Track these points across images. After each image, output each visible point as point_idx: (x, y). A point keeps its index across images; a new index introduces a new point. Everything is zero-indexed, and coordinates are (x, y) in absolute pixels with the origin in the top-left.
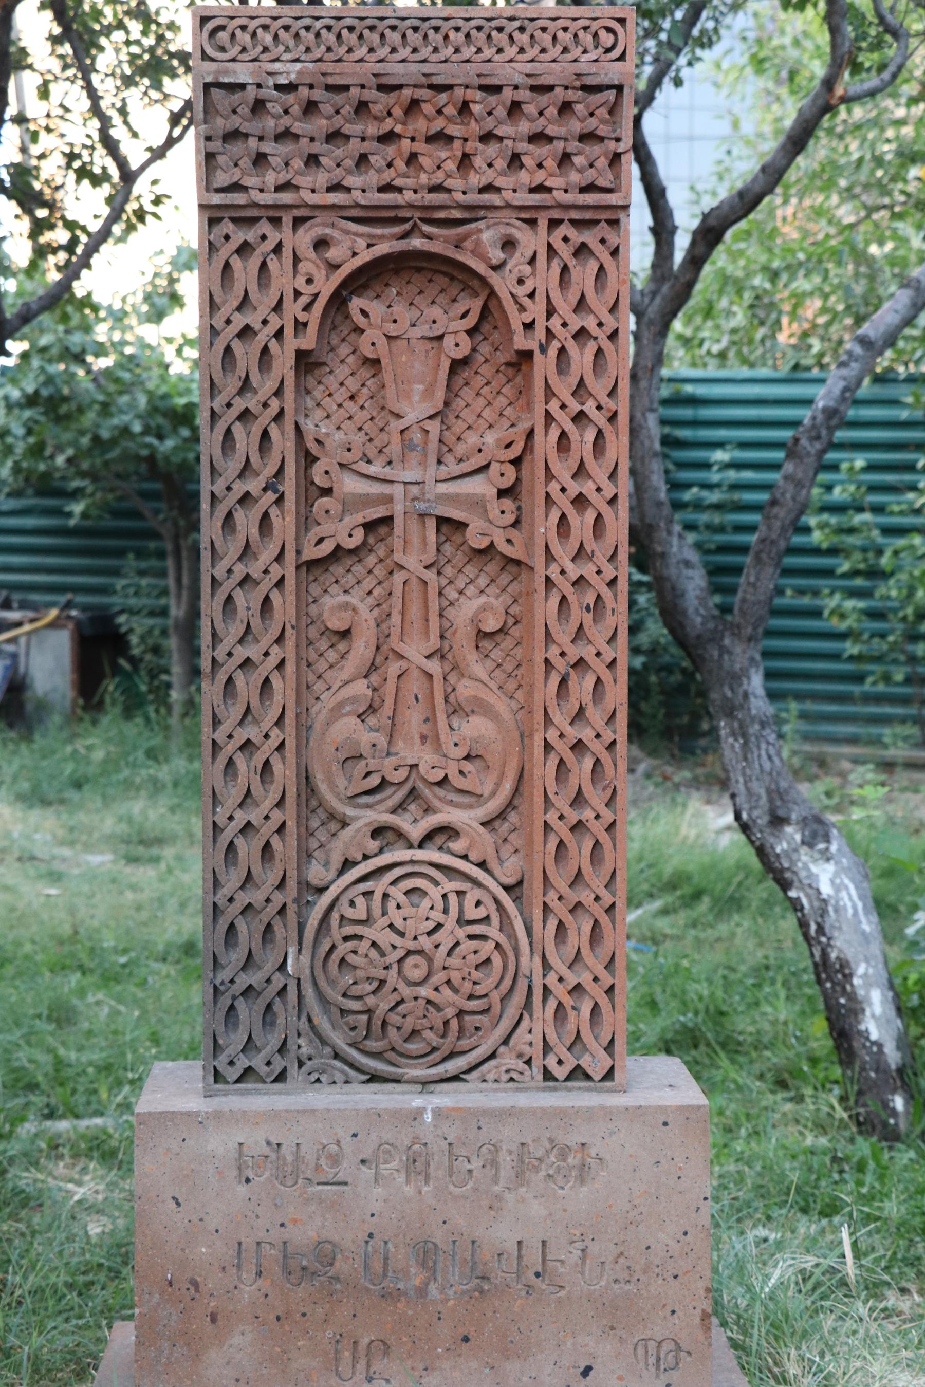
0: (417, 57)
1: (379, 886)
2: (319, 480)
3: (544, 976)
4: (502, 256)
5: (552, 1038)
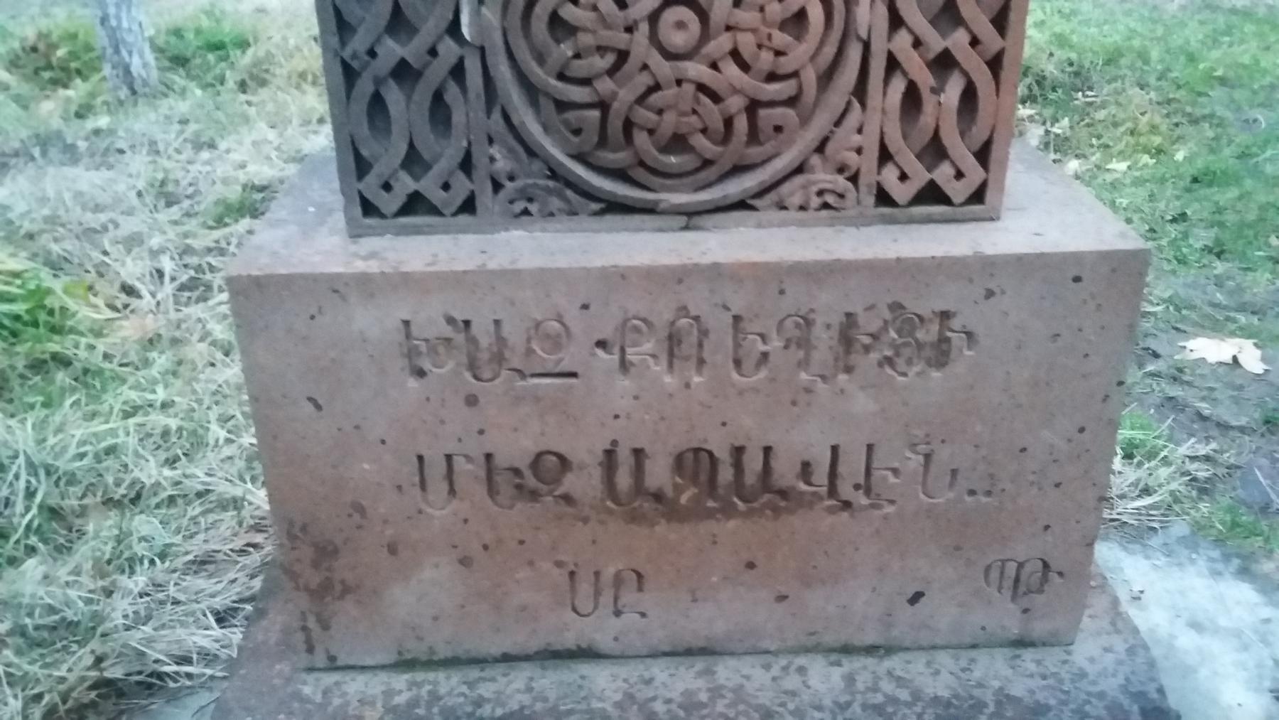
3: (889, 39)
5: (895, 142)
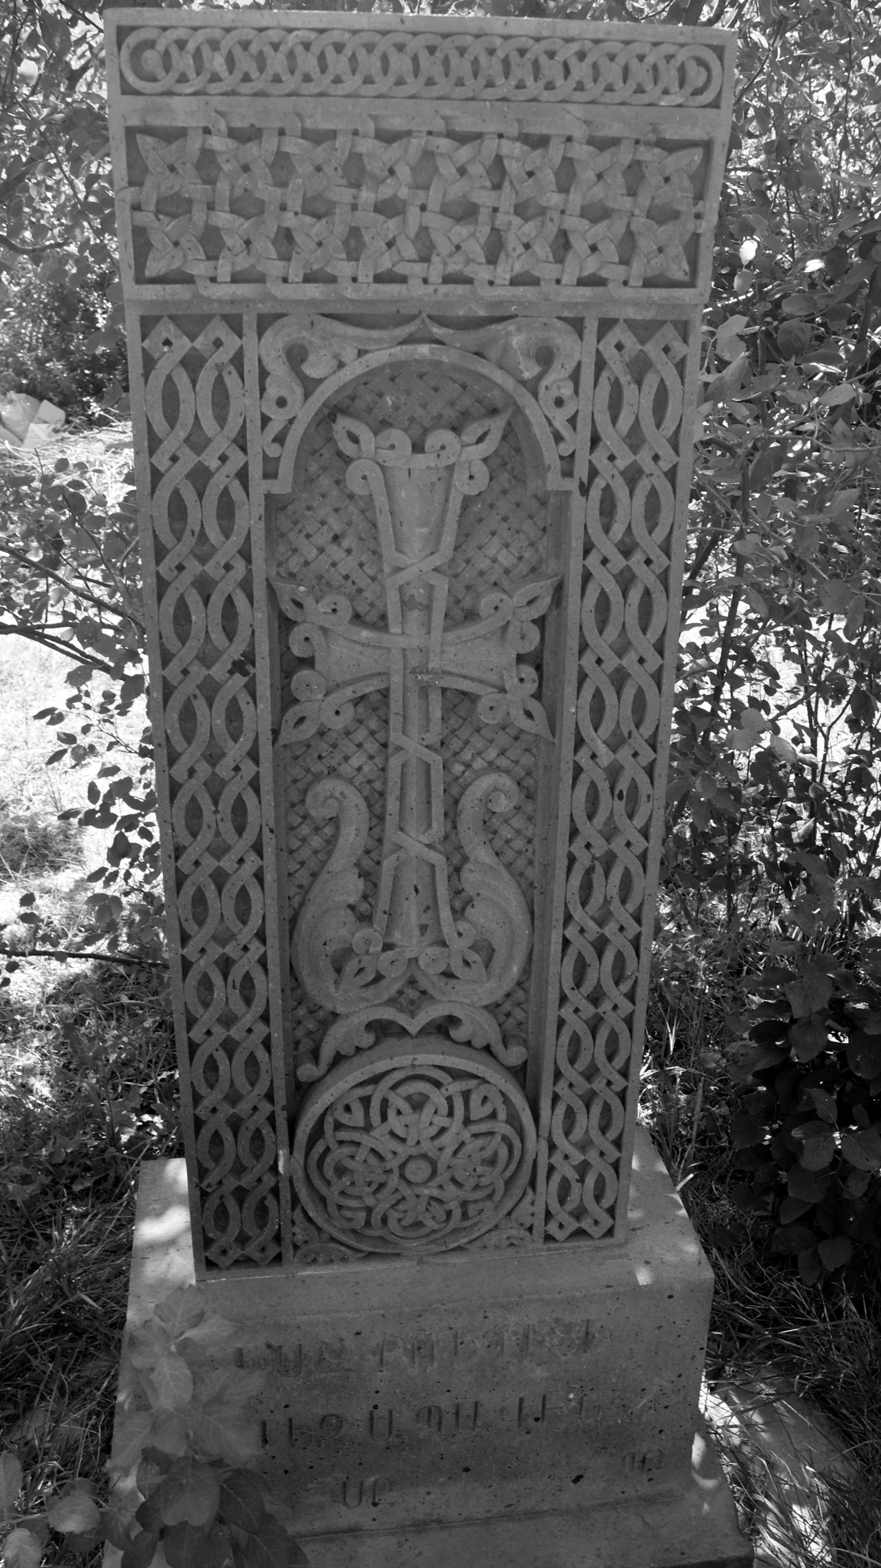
0: (435, 91)
1: (378, 1093)
2: (297, 649)
4: (537, 369)
5: (554, 1205)
